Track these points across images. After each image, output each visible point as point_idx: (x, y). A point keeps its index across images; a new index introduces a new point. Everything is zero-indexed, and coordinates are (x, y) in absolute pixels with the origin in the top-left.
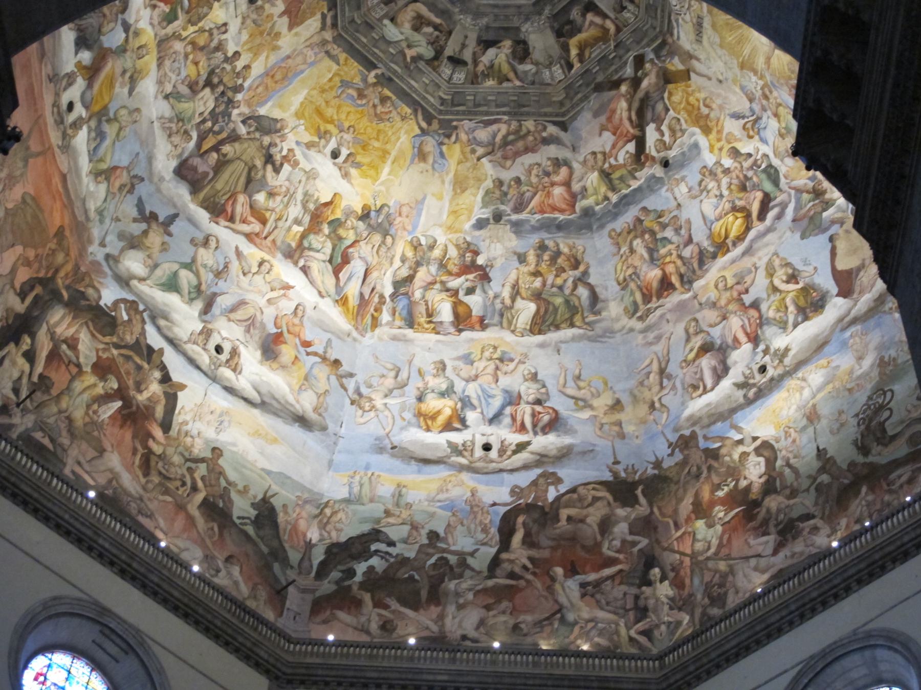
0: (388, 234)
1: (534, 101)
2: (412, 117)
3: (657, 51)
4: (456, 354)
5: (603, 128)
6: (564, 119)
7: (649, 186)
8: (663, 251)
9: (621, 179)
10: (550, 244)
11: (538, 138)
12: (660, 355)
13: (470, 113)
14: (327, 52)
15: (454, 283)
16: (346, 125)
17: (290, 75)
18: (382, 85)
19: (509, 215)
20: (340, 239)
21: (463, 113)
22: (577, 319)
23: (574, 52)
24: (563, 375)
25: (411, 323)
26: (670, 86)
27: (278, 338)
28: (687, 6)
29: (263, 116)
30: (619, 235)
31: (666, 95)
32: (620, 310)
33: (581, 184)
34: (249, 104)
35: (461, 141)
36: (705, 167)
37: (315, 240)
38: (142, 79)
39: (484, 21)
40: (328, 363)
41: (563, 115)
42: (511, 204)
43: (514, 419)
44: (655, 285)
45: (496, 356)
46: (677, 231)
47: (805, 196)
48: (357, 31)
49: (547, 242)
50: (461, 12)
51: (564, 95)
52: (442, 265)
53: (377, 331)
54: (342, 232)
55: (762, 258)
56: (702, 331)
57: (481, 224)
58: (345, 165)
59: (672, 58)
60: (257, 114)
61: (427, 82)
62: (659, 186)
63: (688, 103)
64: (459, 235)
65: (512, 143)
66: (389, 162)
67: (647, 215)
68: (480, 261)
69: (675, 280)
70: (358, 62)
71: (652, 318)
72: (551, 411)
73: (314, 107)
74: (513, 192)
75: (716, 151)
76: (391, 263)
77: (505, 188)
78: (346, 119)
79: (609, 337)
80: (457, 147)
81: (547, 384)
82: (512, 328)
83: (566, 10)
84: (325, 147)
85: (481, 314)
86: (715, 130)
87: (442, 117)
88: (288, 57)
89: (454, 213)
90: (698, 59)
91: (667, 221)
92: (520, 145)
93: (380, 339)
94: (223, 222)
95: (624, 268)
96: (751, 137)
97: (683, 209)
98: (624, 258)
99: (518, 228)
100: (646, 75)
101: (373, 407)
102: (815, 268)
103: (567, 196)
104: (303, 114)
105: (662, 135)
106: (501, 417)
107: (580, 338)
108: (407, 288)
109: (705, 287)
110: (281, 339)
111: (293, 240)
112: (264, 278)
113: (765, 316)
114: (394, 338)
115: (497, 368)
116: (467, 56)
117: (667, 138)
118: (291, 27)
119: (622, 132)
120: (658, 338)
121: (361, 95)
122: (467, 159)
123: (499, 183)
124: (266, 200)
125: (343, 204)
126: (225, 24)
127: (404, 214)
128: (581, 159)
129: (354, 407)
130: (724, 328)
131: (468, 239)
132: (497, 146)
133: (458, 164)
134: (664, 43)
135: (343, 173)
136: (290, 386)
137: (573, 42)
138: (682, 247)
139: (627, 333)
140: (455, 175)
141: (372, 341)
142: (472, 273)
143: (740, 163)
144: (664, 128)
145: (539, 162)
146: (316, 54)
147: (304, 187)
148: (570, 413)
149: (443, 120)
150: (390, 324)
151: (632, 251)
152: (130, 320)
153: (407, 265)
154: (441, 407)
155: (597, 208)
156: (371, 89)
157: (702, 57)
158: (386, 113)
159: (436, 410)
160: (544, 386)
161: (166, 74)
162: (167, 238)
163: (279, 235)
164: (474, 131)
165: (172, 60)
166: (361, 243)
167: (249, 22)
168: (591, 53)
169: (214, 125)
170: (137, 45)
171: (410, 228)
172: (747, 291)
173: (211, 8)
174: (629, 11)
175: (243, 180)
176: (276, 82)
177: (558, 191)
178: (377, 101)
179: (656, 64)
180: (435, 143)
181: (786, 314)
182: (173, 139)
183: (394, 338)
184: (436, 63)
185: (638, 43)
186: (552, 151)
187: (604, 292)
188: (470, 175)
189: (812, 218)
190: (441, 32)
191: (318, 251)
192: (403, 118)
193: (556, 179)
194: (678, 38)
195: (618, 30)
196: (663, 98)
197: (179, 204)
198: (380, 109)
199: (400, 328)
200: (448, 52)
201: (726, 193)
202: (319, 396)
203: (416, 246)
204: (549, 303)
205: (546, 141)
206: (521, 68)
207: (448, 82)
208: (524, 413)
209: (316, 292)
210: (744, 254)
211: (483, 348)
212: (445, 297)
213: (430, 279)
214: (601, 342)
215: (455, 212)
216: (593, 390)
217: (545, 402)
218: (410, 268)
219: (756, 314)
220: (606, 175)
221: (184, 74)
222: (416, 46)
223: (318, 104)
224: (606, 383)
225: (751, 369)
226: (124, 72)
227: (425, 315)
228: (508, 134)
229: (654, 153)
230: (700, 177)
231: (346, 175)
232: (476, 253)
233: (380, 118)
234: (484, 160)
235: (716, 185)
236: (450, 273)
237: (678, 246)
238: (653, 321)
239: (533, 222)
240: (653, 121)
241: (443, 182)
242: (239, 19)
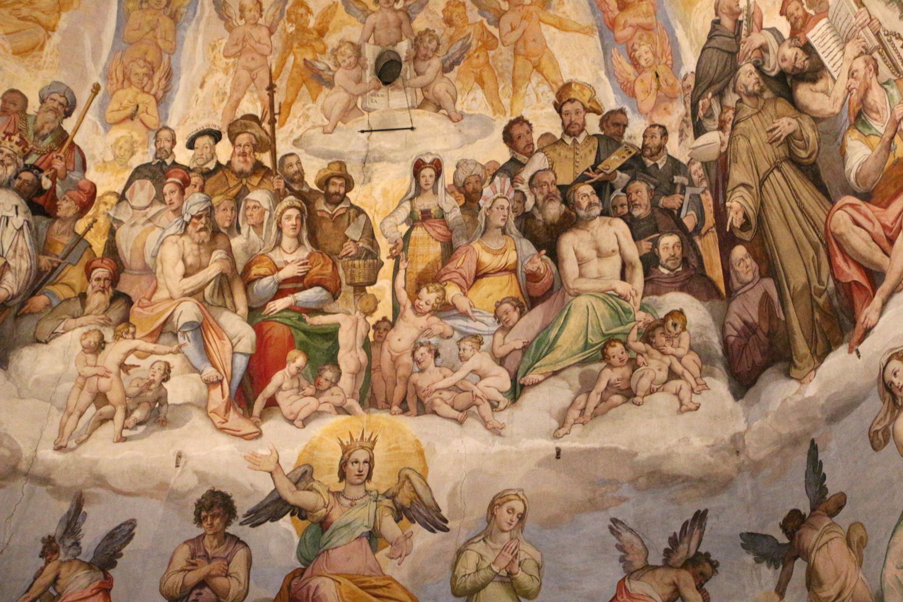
29: (699, 62)
34: (665, 98)
38: (423, 477)
60: (691, 81)
94: (868, 314)
126: (418, 166)
161: (455, 388)
162: (843, 518)
165: (429, 358)
167: (440, 88)
169: (679, 227)
170: (332, 480)
173: (360, 211)
175: (807, 193)
182: (645, 383)
197: (797, 428)
221: (485, 325)
226: (374, 537)
242: (426, 119)
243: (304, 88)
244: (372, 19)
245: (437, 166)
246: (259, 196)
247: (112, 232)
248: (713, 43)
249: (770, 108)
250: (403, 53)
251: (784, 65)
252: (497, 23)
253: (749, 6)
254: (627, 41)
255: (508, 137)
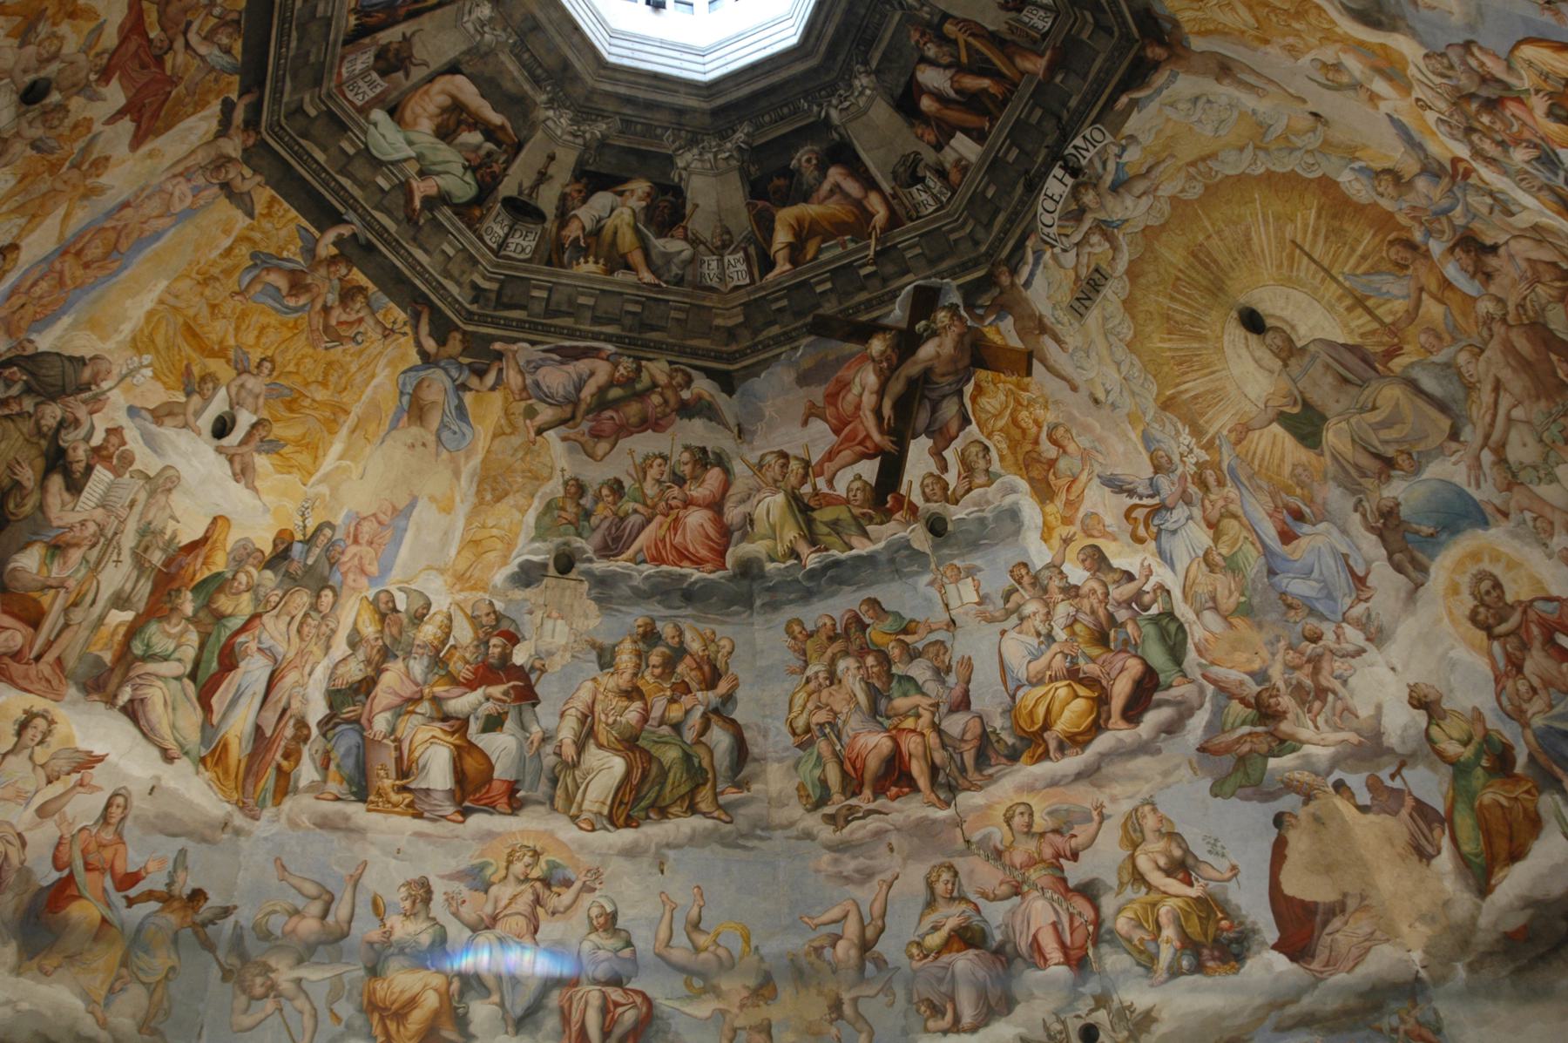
0: (323, 588)
1: (678, 320)
2: (407, 329)
3: (970, 293)
4: (453, 865)
5: (812, 413)
6: (731, 367)
7: (892, 561)
8: (901, 703)
9: (834, 525)
10: (666, 629)
11: (672, 401)
12: (865, 910)
13: (533, 327)
14: (226, 187)
15: (462, 703)
16: (255, 356)
17: (123, 247)
18: (350, 263)
19: (590, 560)
20: (220, 617)
21: (520, 325)
22: (704, 799)
23: (782, 237)
24: (667, 916)
25: (361, 789)
26: (983, 375)
27: (63, 891)
28: (1077, 238)
30: (810, 635)
31: (969, 389)
32: (791, 787)
33: (742, 509)
35: (507, 387)
36: (1025, 565)
37: (158, 636)
39: (600, 128)
40: (176, 904)
41: (731, 358)
42: (597, 538)
43: (565, 1018)
44: (873, 764)
45: (536, 873)
46: (941, 673)
47: (1236, 706)
48: (305, 136)
49: (659, 625)
50: (551, 103)
51: (741, 319)
52: (438, 661)
53: (288, 804)
54: (224, 603)
55: (1119, 799)
56: (963, 898)
57: (528, 576)
58: (245, 449)
59: (1000, 318)
60: (30, 351)
61: (451, 252)
62: (915, 568)
63: (1015, 422)
64: (480, 594)
65: (615, 404)
66: (344, 431)
67: (877, 618)
68: (520, 657)
69: (917, 769)
70: (297, 210)
71: (858, 830)
72: (639, 1000)
73: (180, 320)
74: (602, 511)
75: (1056, 542)
76: (328, 648)
77: (586, 502)
78: (257, 344)
79: (761, 838)
80: (497, 398)
81: (634, 941)
82: (574, 811)
83: (787, 144)
84: (198, 414)
85: (511, 776)
86: (1064, 496)
87: (470, 328)
88: (126, 205)
89: (473, 544)
90: (1058, 340)
91: (920, 646)
92: (633, 410)
93: (293, 824)
95: (810, 706)
96: (1141, 541)
97: (959, 632)
98: (812, 685)
99: (604, 588)
100: (935, 334)
101: (272, 989)
102: (1234, 868)
103: (712, 533)
104: (153, 341)
105: (945, 468)
106: (540, 1014)
107: (705, 838)
108: (358, 708)
109: (984, 812)
110: (71, 891)
111: (106, 647)
112: (31, 758)
113: (1107, 925)
114: (324, 823)
115: (537, 901)
116: (547, 200)
117: (952, 477)
118: (137, 142)
119: (854, 433)
120: (866, 875)
121: (297, 285)
122: (514, 429)
123: (578, 488)
124: (43, 563)
125: (233, 537)
127: (364, 538)
128: (754, 458)
129: (229, 985)
130: (1013, 912)
131: (499, 606)
132: (583, 407)
133: (495, 436)
134: (989, 281)
135: (238, 470)
136: (86, 996)
137: (785, 217)
138: (943, 709)
139: (798, 838)
140: (484, 461)
141: (275, 828)
142: (499, 682)
143: (1105, 585)
144: (949, 454)
145: (667, 452)
146: (197, 191)
147: (142, 515)
148: (676, 1004)
149: (473, 334)
150: (316, 789)
151: (832, 678)
153: (361, 655)
154: (417, 989)
155: (770, 567)
156: (323, 271)
157: (1072, 341)
158: (350, 324)
159: (407, 996)
160: (629, 944)
163: (72, 647)
164: (537, 368)
166: (265, 618)
168: (819, 251)
171: (373, 569)
172: (1075, 856)
174: (927, 189)
176: (86, 266)
177: (696, 519)
178: (332, 298)
179: (961, 318)
180: (448, 384)
181: (1155, 940)
183: (324, 823)
184: (477, 213)
185: (932, 262)
186: (697, 431)
187: (760, 739)
188: (518, 465)
189: (1242, 759)
190: (498, 143)
191: (166, 659)
192: (387, 333)
193: (696, 492)
194: (1027, 284)
195: (894, 221)
196: (960, 393)
198: (337, 315)
199: (337, 799)
200: (507, 188)
201: (1061, 635)
202: (151, 989)
203: (384, 612)
204: (649, 758)
205: (687, 410)
206: (661, 245)
207: (496, 253)
208: (587, 1003)
209: (155, 753)
210: (1079, 776)
211: (510, 855)
212: (439, 733)
213: (409, 690)
214: (744, 847)
215: (477, 543)
216: (721, 952)
217: (629, 980)
218: (368, 662)
219: (1089, 913)
220: (802, 508)
222: (438, 174)
223: (191, 312)
224: (747, 940)
225: (1063, 1023)
227: (393, 774)
228: (611, 384)
229: (916, 498)
230: (1009, 582)
231: (243, 473)
232: (513, 639)
233: (334, 335)
234: (551, 435)
235: (1043, 610)
236: (453, 680)
237: (936, 705)
238: (859, 835)
239: (637, 581)
240: (929, 434)
241: (457, 474)
243: (19, 19)
244: (82, 57)
248: (67, 363)
249: (34, 452)
250: (47, 101)
251: (70, 452)
252: (74, 166)
253: (104, 393)
254: (51, 271)
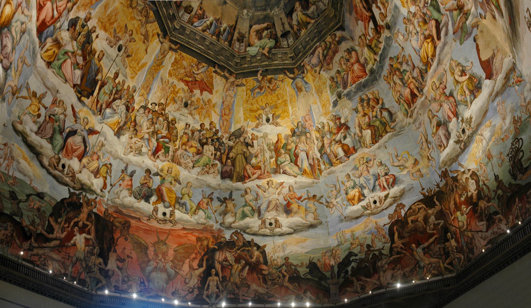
10: (364, 97)
57: (335, 104)
88: (223, 102)
126: (187, 124)
152: (238, 238)
239: (354, 90)
241: (313, 95)
245: (189, 125)
246: (161, 119)
247: (135, 117)
255: (201, 125)
